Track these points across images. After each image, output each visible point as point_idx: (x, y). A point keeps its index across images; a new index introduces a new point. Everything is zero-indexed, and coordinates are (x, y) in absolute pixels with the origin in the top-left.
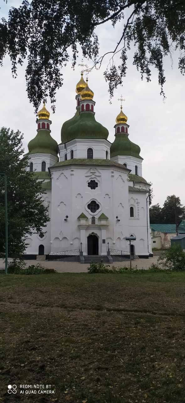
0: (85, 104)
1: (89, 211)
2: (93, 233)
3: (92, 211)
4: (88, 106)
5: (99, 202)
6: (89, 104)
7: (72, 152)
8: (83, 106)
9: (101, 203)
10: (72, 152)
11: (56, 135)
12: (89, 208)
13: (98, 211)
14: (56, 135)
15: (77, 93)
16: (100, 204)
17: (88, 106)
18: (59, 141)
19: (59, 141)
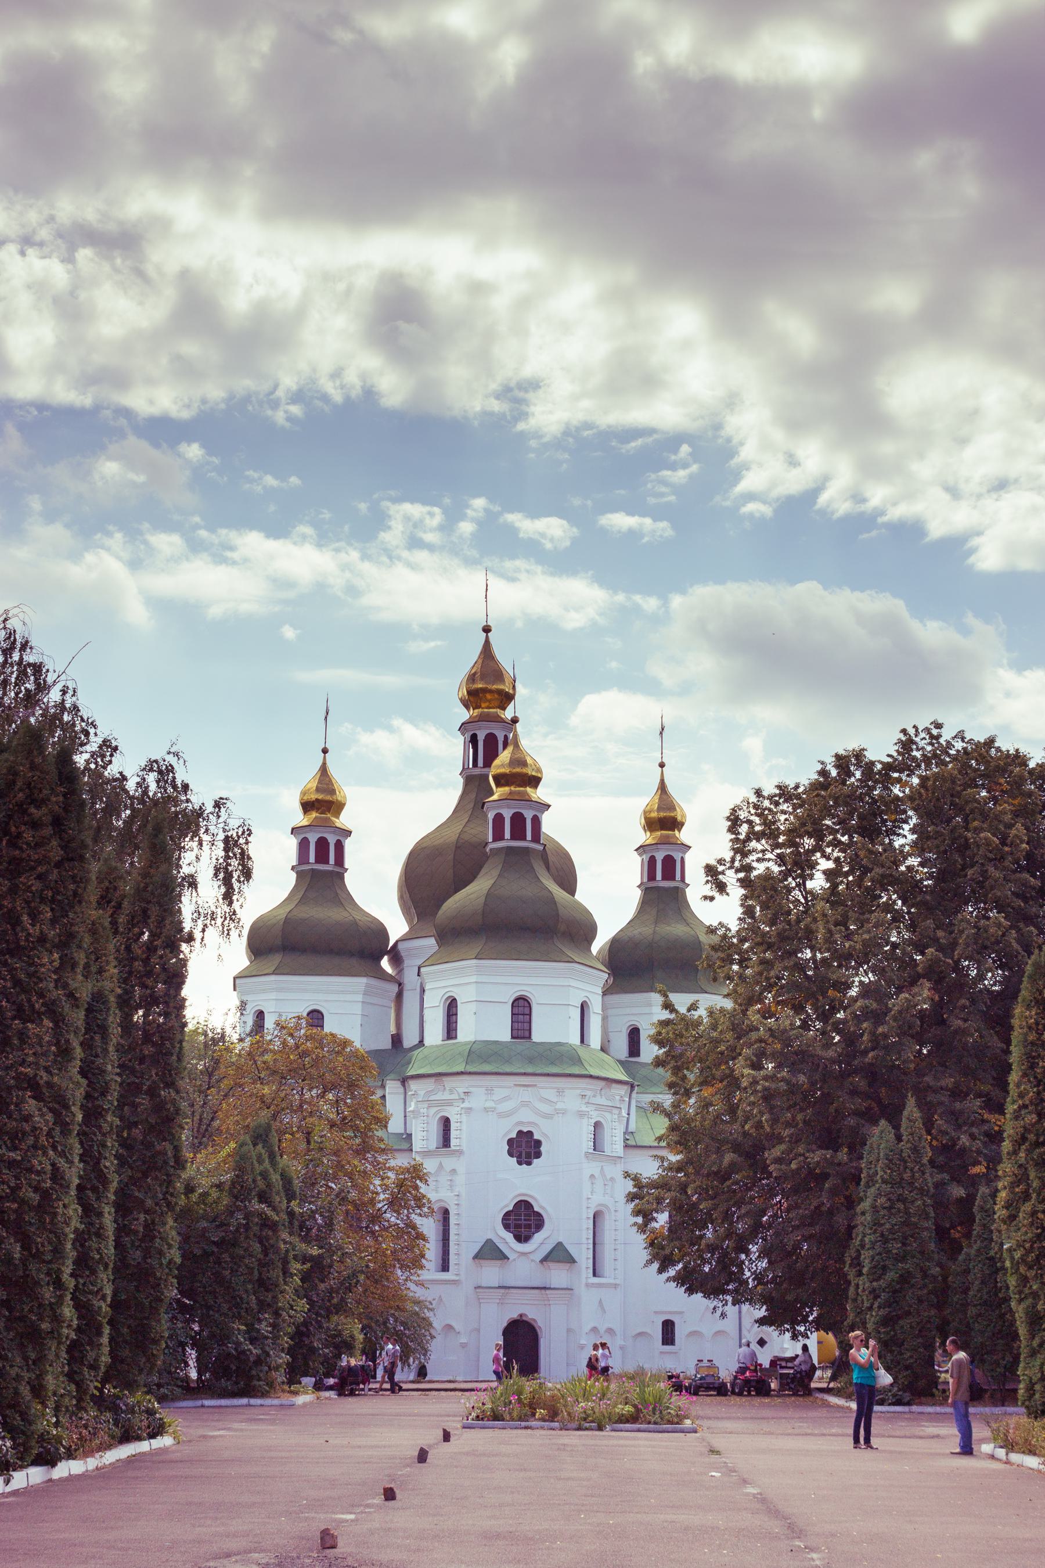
0: (507, 814)
1: (509, 1237)
2: (521, 1315)
3: (519, 1238)
4: (518, 820)
5: (542, 1207)
6: (522, 814)
7: (451, 1008)
8: (499, 819)
9: (549, 1209)
10: (451, 1008)
11: (375, 889)
12: (507, 1227)
13: (538, 1237)
14: (375, 889)
15: (467, 707)
16: (546, 1211)
17: (518, 820)
18: (397, 926)
19: (397, 926)
